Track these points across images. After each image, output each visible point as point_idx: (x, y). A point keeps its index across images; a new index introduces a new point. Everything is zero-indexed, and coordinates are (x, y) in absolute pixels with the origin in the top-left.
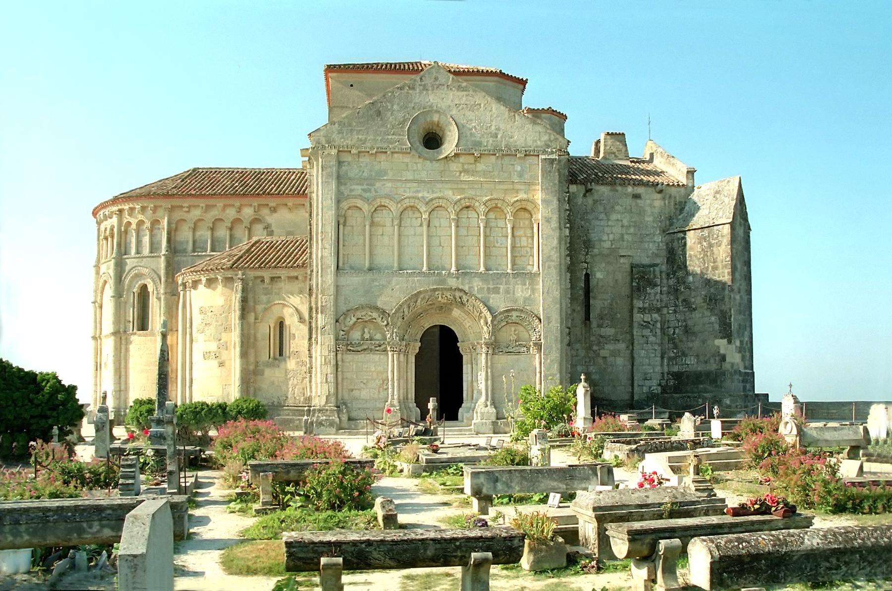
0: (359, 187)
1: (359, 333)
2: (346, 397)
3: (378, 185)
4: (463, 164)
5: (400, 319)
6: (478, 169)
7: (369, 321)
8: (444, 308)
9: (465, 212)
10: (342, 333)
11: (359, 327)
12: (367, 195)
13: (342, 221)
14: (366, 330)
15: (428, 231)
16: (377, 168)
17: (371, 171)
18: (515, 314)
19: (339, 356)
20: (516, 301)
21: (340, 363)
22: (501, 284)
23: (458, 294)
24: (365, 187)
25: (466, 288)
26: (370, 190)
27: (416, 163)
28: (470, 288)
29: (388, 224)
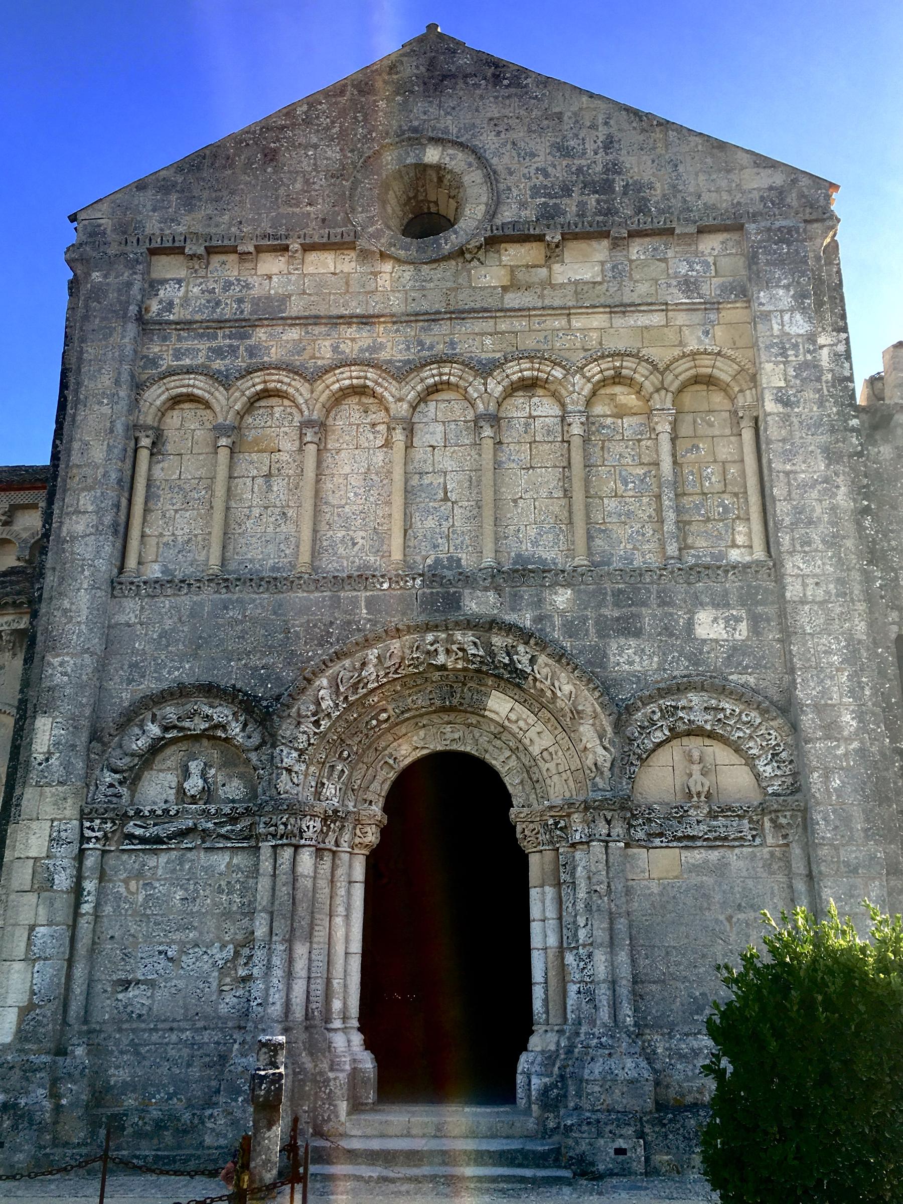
0: (203, 346)
1: (171, 779)
2: (105, 1009)
3: (261, 334)
4: (512, 270)
5: (307, 726)
6: (559, 279)
7: (203, 735)
8: (455, 693)
9: (519, 400)
10: (109, 777)
11: (172, 757)
12: (218, 365)
13: (145, 442)
14: (195, 767)
15: (407, 460)
16: (255, 292)
17: (240, 301)
18: (695, 699)
19: (90, 861)
20: (695, 659)
21: (89, 885)
22: (644, 604)
23: (498, 641)
24: (222, 341)
25: (526, 619)
26: (233, 350)
27: (375, 274)
28: (539, 619)
29: (288, 445)
